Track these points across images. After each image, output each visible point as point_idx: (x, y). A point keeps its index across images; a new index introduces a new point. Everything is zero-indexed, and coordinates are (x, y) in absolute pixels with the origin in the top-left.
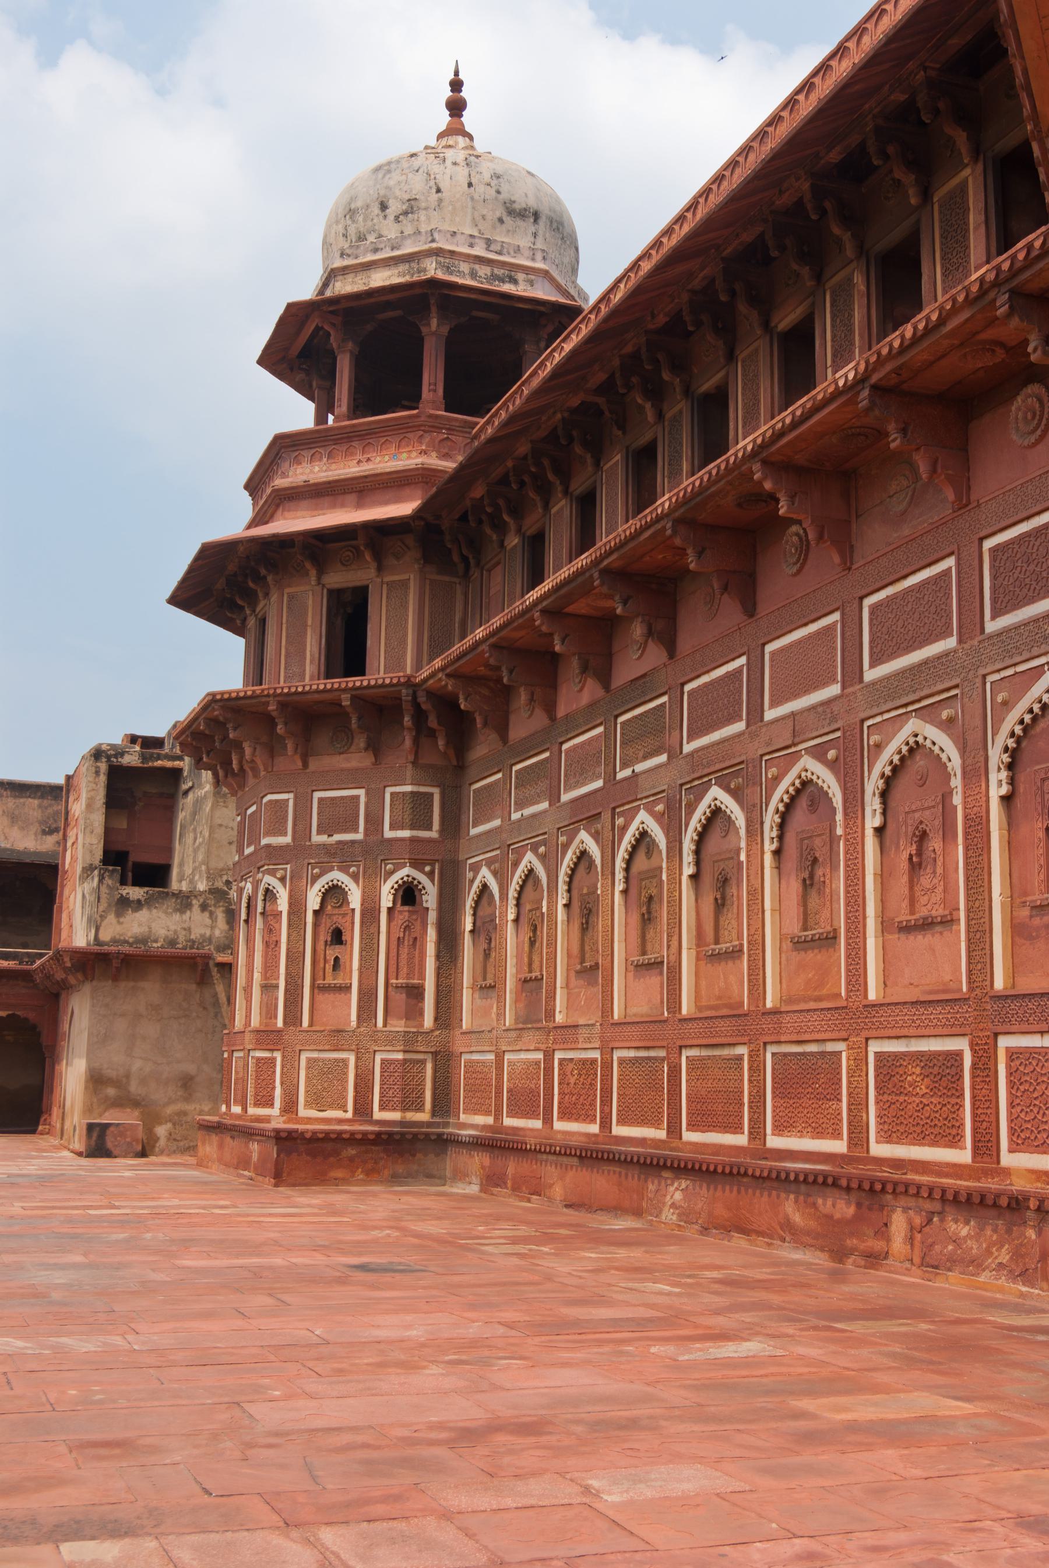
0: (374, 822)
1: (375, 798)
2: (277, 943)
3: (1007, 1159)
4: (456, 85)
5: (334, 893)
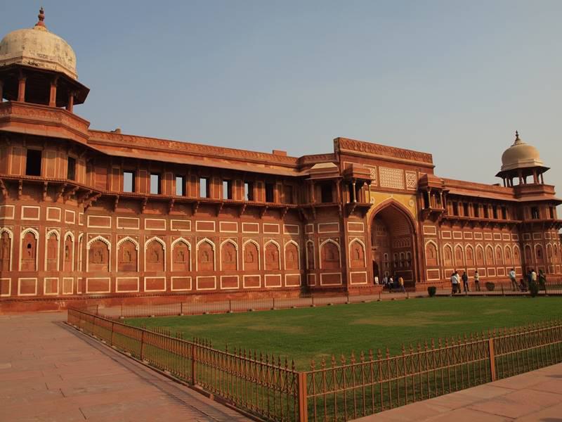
1: (77, 214)
4: (41, 12)
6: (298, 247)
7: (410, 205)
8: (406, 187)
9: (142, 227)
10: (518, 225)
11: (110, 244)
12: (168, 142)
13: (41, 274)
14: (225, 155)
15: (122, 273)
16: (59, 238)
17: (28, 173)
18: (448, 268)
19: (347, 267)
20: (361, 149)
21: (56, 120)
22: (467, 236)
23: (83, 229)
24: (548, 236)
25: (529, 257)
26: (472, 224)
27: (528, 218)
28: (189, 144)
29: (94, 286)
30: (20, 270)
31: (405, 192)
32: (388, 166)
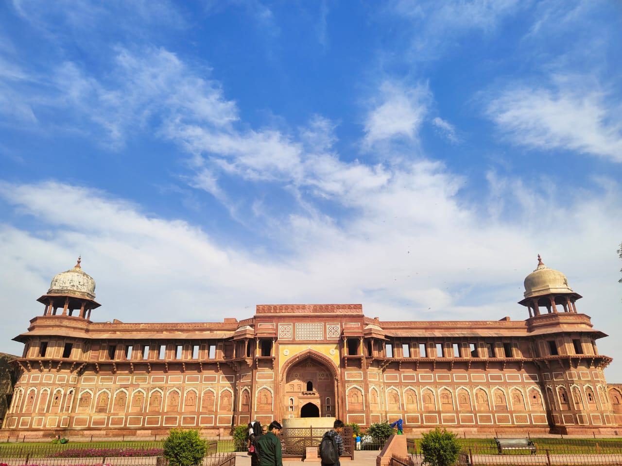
0: (68, 381)
2: (46, 399)
3: (200, 425)
4: (80, 259)
7: (332, 354)
8: (325, 337)
9: (115, 383)
10: (532, 363)
11: (92, 394)
13: (33, 415)
14: (179, 328)
15: (96, 414)
18: (410, 413)
19: (252, 410)
20: (278, 311)
21: (58, 323)
22: (440, 378)
23: (71, 386)
24: (571, 376)
25: (552, 401)
26: (447, 365)
29: (80, 422)
30: (23, 412)
31: (325, 342)
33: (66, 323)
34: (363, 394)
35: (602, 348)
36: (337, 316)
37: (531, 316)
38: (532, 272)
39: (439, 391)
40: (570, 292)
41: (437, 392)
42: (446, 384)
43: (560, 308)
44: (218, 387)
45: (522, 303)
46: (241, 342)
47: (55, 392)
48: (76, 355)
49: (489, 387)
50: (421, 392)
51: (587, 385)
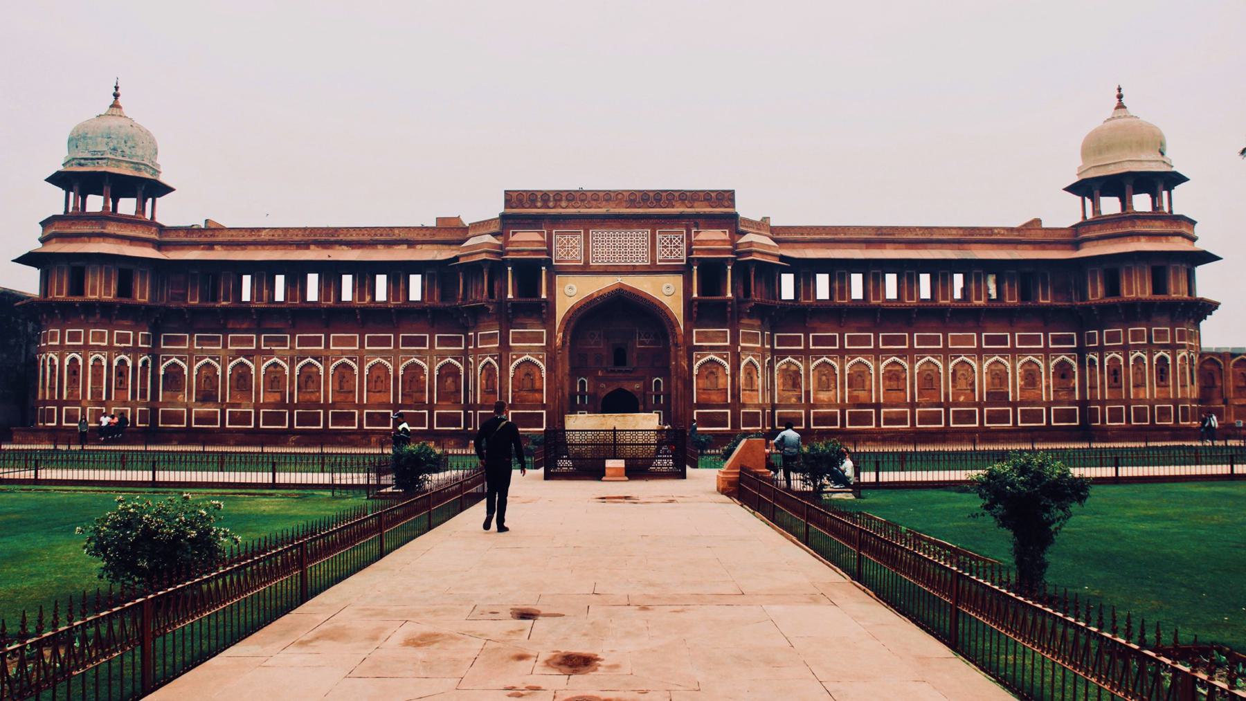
0: (136, 341)
1: (136, 335)
4: (117, 88)
5: (122, 362)
6: (462, 369)
7: (668, 292)
8: (653, 260)
9: (225, 346)
12: (259, 229)
13: (84, 403)
14: (341, 237)
16: (105, 363)
17: (72, 292)
18: (822, 407)
20: (551, 204)
21: (98, 230)
22: (887, 341)
24: (1136, 336)
25: (1093, 387)
27: (1096, 293)
28: (287, 229)
29: (168, 417)
30: (65, 397)
31: (653, 270)
32: (611, 227)
33: (112, 229)
34: (728, 372)
35: (1206, 282)
36: (681, 217)
37: (1084, 217)
38: (1101, 123)
39: (882, 367)
40: (1164, 169)
41: (877, 370)
42: (901, 354)
43: (1142, 203)
44: (431, 357)
45: (1073, 189)
46: (474, 269)
47: (115, 363)
48: (142, 294)
49: (980, 359)
50: (847, 368)
51: (1162, 353)
